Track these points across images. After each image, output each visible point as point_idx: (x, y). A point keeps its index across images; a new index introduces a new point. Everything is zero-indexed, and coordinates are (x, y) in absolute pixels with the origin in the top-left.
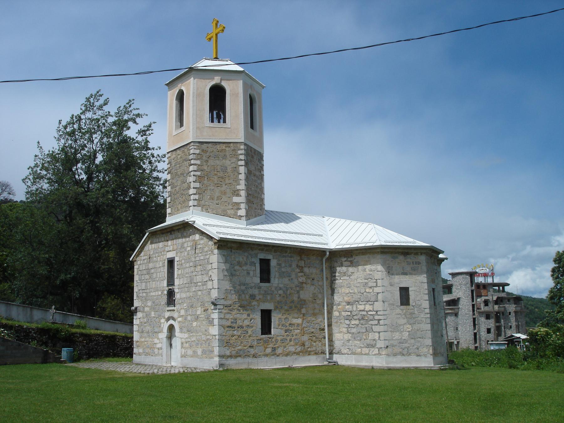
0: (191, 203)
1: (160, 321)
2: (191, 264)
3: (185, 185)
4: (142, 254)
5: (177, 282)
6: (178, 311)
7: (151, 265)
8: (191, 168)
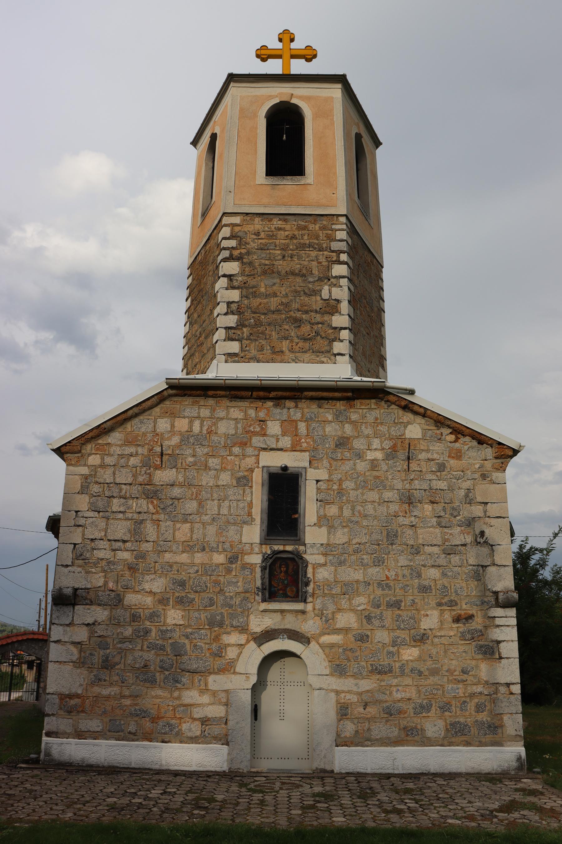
0: (338, 347)
1: (217, 638)
2: (388, 495)
3: (316, 303)
4: (115, 437)
5: (313, 535)
6: (321, 615)
7: (163, 476)
8: (340, 270)
